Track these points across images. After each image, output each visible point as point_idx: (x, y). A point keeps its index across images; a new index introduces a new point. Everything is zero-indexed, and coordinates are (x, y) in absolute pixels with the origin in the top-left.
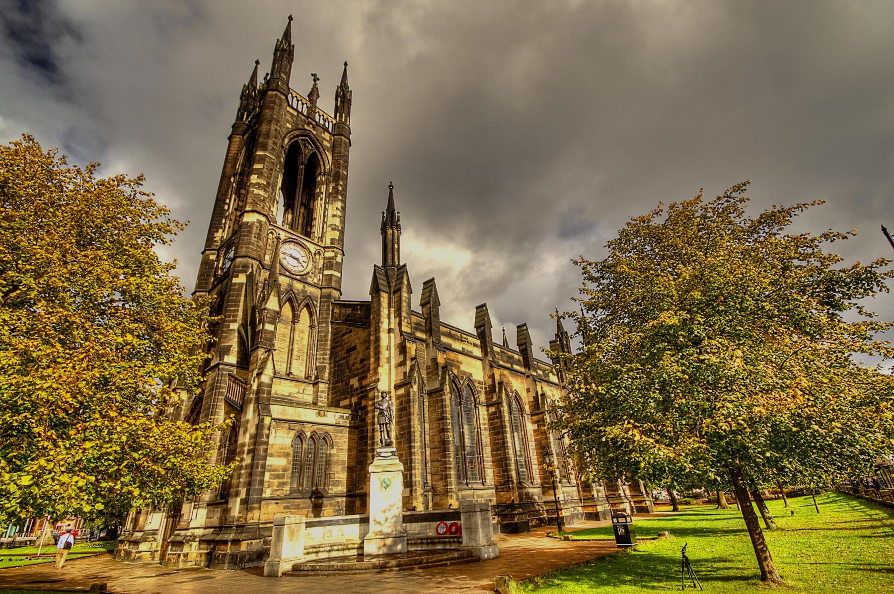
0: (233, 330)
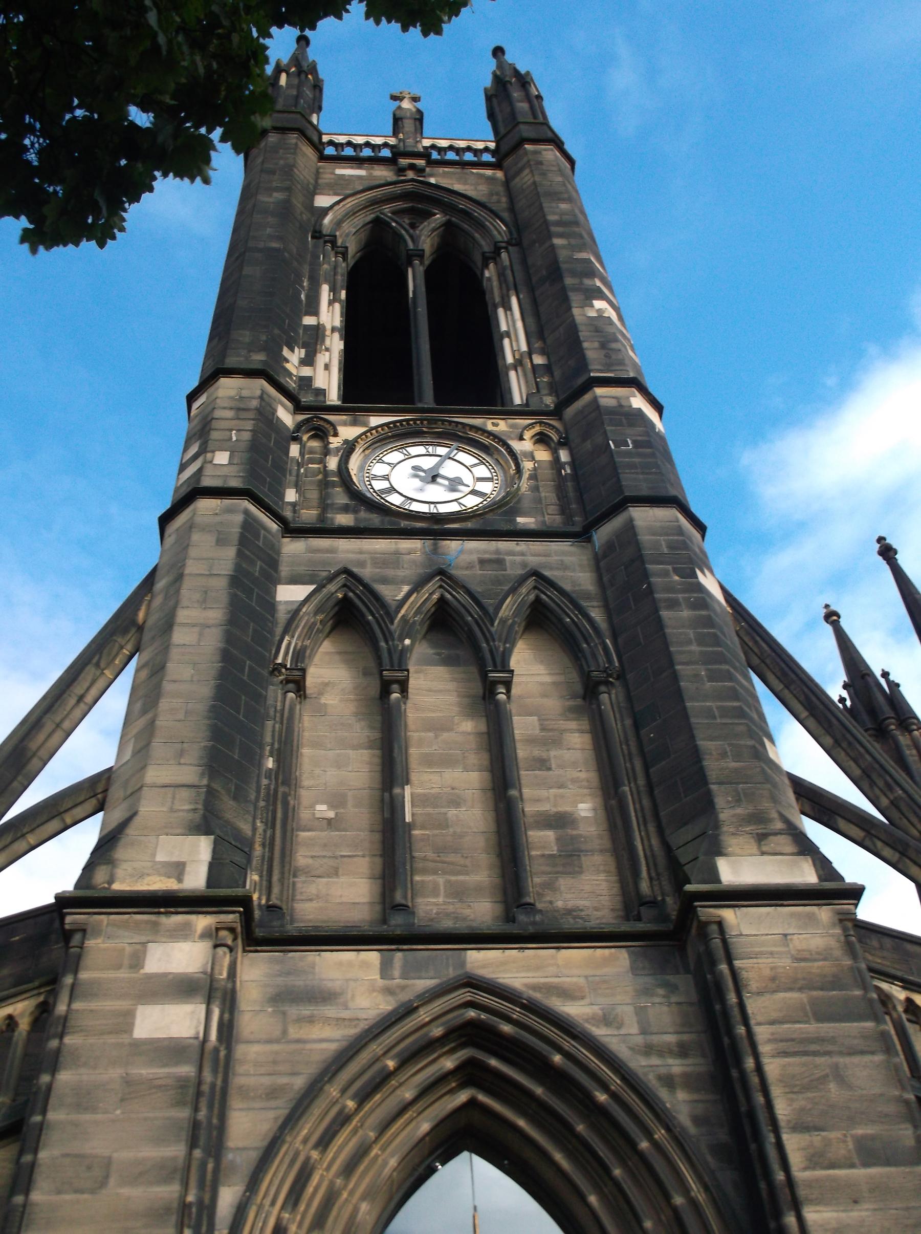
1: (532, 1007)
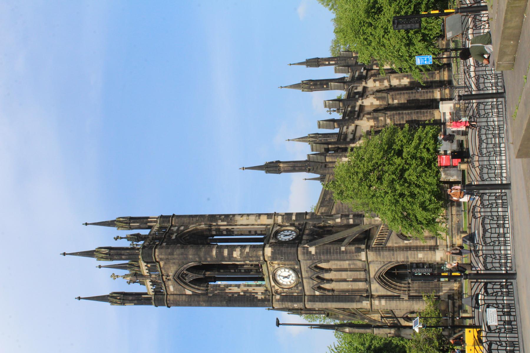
0: (346, 249)
1: (377, 272)
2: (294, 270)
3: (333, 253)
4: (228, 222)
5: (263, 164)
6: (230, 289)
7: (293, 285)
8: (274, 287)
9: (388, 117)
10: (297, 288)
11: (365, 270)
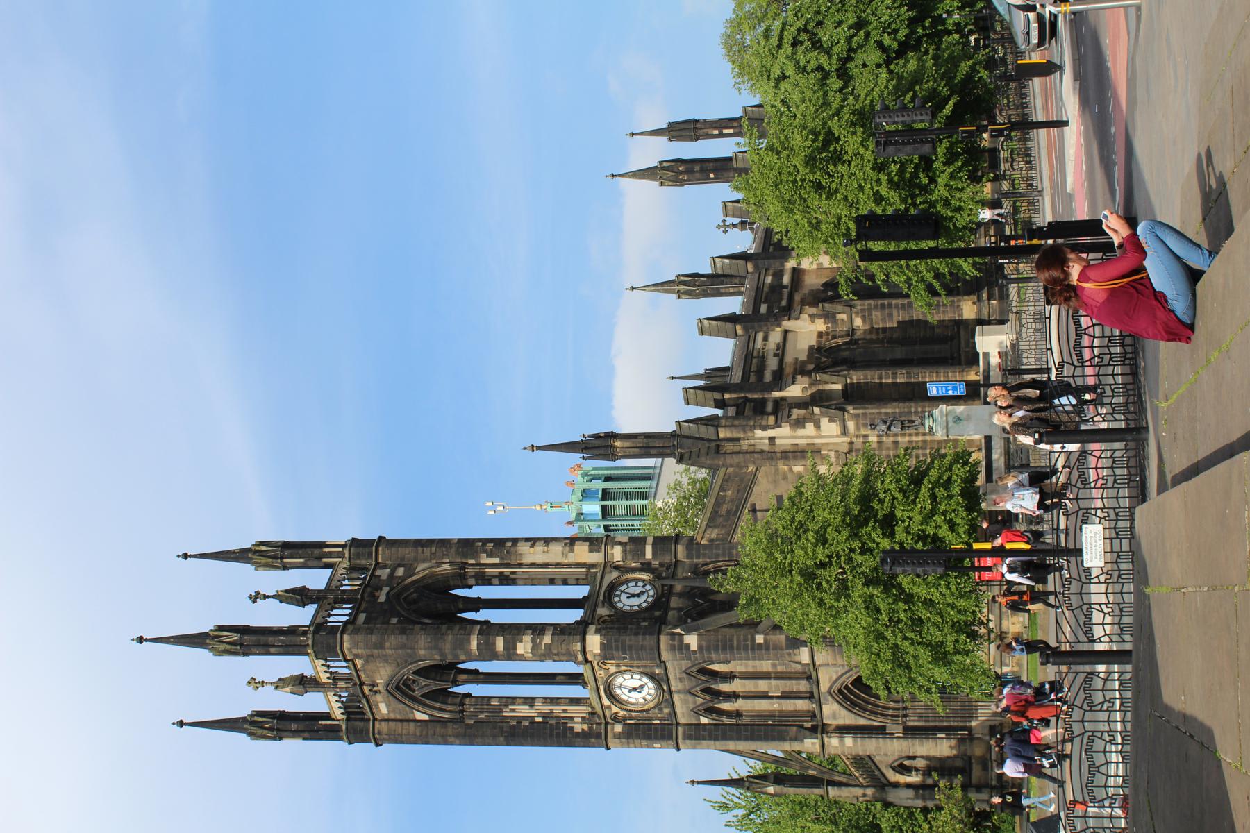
2: (652, 677)
3: (739, 649)
4: (502, 559)
5: (577, 438)
6: (513, 711)
7: (651, 705)
8: (609, 707)
9: (857, 313)
10: (661, 710)
11: (809, 678)
